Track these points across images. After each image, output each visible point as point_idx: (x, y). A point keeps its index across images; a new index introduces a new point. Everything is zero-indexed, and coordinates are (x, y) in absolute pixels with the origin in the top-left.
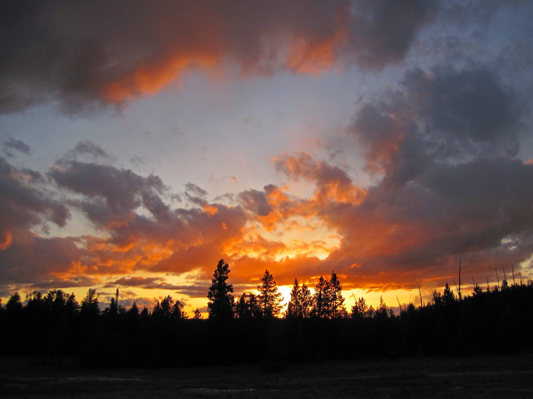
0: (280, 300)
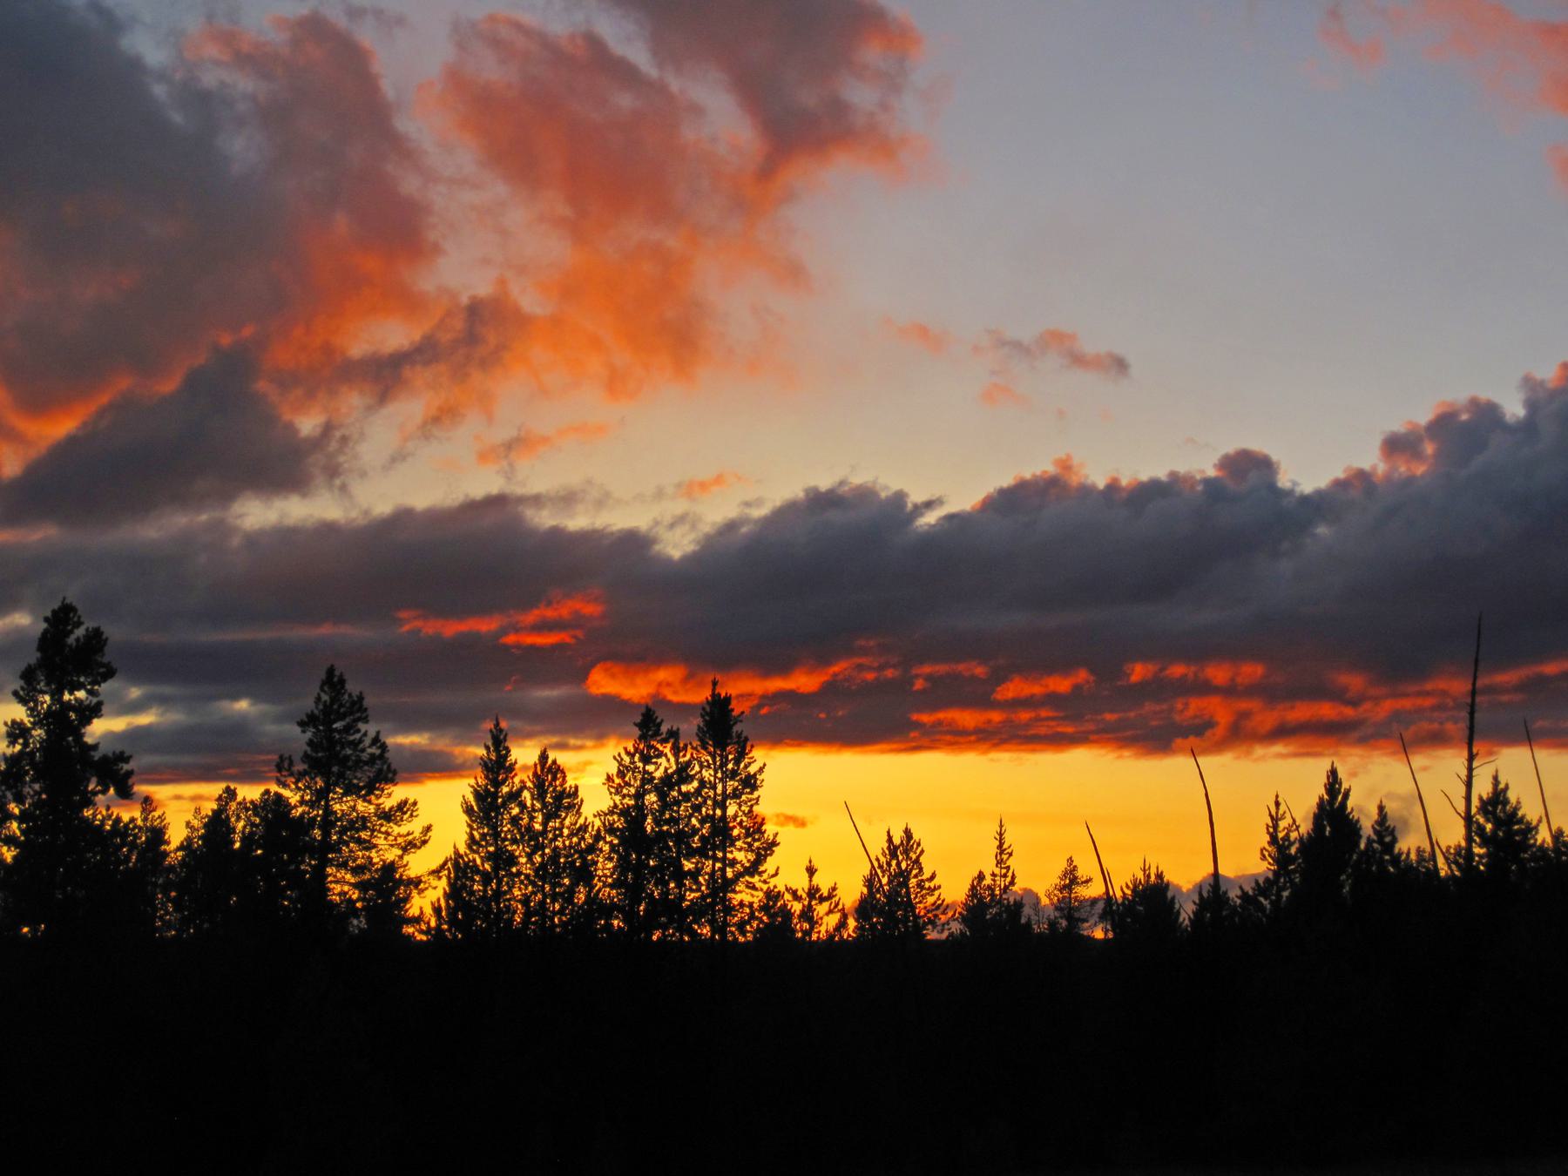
0: (410, 846)
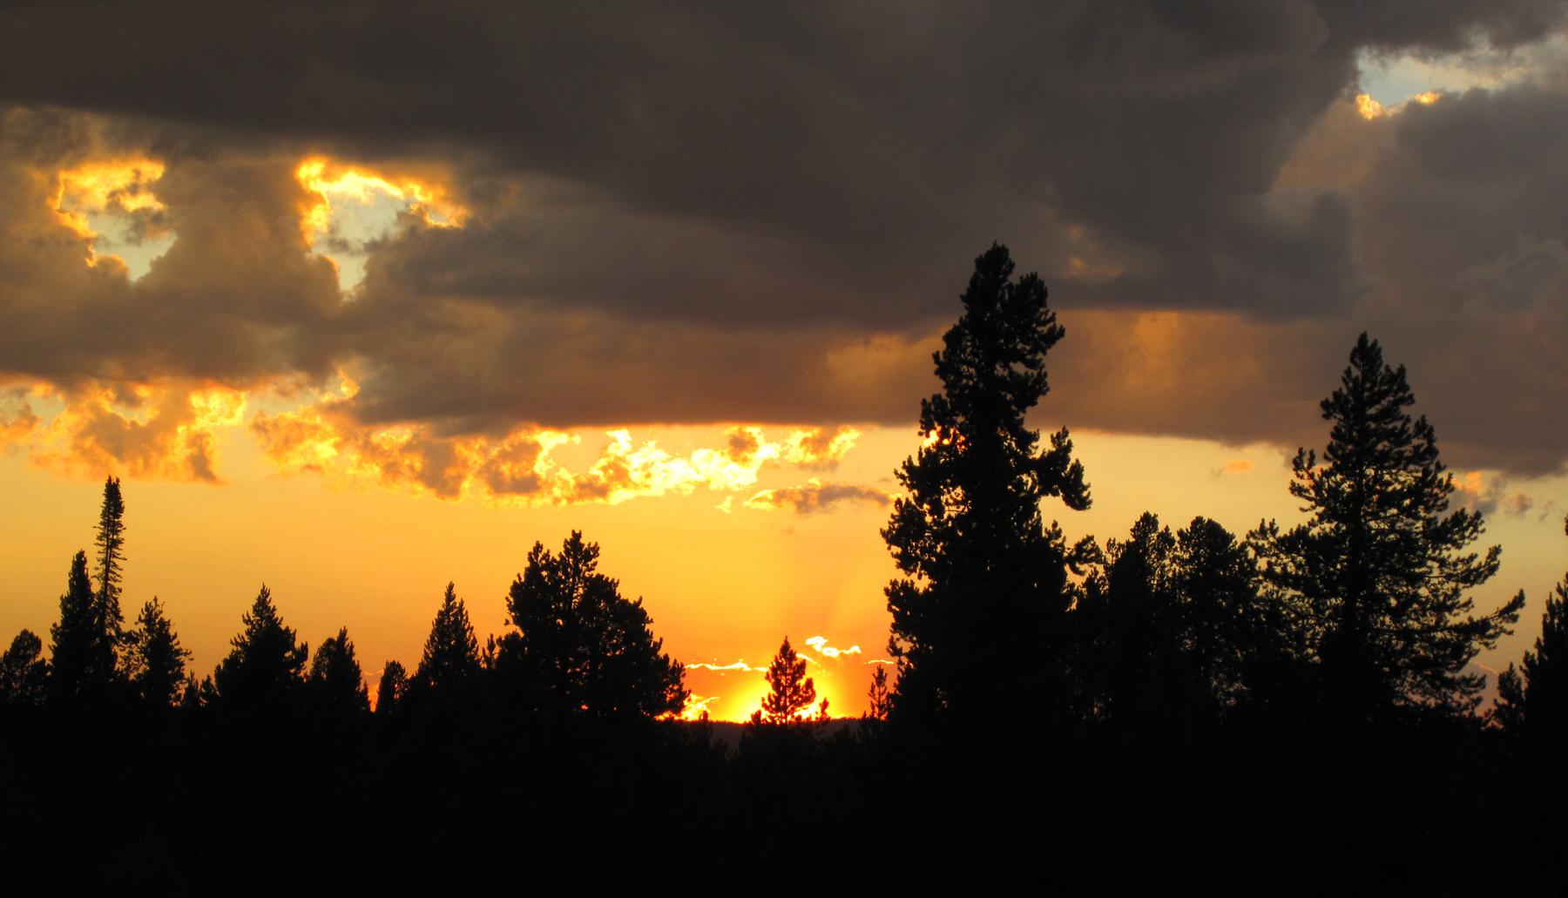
0: (1474, 576)
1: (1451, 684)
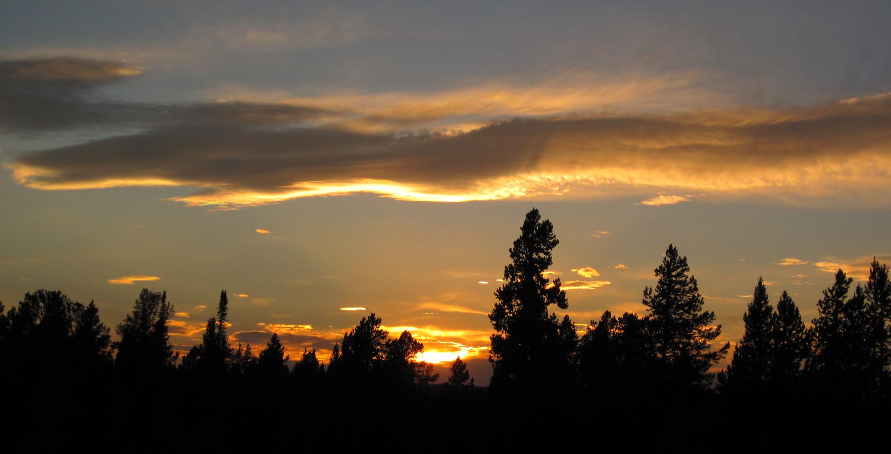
0: (711, 336)
1: (703, 377)
